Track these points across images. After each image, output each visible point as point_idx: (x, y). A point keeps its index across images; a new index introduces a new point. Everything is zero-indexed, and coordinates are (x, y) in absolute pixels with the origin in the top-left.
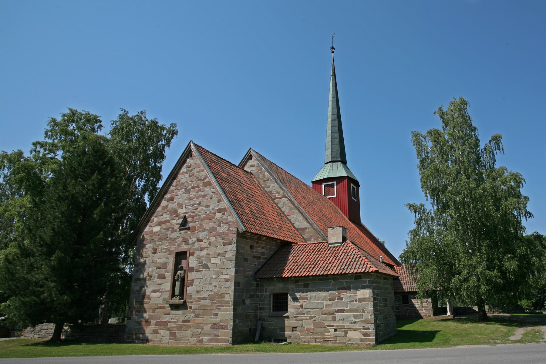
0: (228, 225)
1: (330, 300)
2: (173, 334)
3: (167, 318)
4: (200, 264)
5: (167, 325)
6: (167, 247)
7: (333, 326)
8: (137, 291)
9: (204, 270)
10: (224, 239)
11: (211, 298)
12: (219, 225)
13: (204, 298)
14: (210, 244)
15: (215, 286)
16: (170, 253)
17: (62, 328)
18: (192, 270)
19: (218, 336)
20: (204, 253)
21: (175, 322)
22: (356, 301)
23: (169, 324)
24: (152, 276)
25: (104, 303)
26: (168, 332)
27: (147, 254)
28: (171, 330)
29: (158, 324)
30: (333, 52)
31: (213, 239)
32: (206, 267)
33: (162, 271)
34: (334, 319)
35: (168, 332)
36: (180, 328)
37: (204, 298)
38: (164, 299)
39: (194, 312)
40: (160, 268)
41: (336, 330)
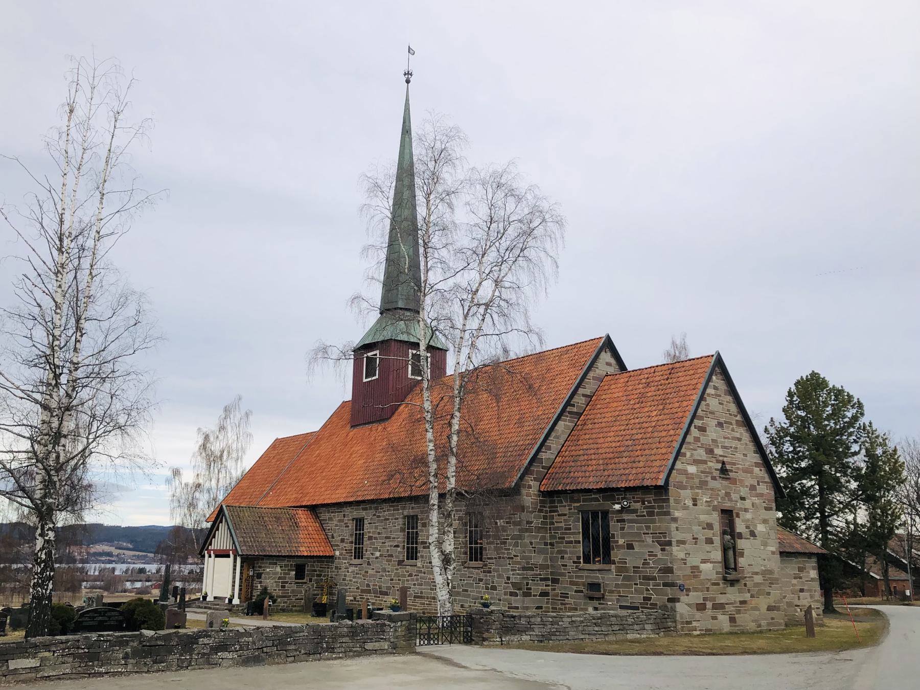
1: (795, 578)
2: (732, 620)
3: (722, 599)
5: (724, 608)
7: (799, 606)
13: (757, 573)
14: (753, 505)
15: (765, 560)
16: (715, 509)
18: (740, 536)
20: (749, 516)
21: (732, 604)
23: (727, 606)
24: (697, 538)
26: (727, 617)
28: (730, 614)
32: (753, 534)
36: (739, 612)
37: (757, 573)
38: (717, 573)
39: (749, 591)
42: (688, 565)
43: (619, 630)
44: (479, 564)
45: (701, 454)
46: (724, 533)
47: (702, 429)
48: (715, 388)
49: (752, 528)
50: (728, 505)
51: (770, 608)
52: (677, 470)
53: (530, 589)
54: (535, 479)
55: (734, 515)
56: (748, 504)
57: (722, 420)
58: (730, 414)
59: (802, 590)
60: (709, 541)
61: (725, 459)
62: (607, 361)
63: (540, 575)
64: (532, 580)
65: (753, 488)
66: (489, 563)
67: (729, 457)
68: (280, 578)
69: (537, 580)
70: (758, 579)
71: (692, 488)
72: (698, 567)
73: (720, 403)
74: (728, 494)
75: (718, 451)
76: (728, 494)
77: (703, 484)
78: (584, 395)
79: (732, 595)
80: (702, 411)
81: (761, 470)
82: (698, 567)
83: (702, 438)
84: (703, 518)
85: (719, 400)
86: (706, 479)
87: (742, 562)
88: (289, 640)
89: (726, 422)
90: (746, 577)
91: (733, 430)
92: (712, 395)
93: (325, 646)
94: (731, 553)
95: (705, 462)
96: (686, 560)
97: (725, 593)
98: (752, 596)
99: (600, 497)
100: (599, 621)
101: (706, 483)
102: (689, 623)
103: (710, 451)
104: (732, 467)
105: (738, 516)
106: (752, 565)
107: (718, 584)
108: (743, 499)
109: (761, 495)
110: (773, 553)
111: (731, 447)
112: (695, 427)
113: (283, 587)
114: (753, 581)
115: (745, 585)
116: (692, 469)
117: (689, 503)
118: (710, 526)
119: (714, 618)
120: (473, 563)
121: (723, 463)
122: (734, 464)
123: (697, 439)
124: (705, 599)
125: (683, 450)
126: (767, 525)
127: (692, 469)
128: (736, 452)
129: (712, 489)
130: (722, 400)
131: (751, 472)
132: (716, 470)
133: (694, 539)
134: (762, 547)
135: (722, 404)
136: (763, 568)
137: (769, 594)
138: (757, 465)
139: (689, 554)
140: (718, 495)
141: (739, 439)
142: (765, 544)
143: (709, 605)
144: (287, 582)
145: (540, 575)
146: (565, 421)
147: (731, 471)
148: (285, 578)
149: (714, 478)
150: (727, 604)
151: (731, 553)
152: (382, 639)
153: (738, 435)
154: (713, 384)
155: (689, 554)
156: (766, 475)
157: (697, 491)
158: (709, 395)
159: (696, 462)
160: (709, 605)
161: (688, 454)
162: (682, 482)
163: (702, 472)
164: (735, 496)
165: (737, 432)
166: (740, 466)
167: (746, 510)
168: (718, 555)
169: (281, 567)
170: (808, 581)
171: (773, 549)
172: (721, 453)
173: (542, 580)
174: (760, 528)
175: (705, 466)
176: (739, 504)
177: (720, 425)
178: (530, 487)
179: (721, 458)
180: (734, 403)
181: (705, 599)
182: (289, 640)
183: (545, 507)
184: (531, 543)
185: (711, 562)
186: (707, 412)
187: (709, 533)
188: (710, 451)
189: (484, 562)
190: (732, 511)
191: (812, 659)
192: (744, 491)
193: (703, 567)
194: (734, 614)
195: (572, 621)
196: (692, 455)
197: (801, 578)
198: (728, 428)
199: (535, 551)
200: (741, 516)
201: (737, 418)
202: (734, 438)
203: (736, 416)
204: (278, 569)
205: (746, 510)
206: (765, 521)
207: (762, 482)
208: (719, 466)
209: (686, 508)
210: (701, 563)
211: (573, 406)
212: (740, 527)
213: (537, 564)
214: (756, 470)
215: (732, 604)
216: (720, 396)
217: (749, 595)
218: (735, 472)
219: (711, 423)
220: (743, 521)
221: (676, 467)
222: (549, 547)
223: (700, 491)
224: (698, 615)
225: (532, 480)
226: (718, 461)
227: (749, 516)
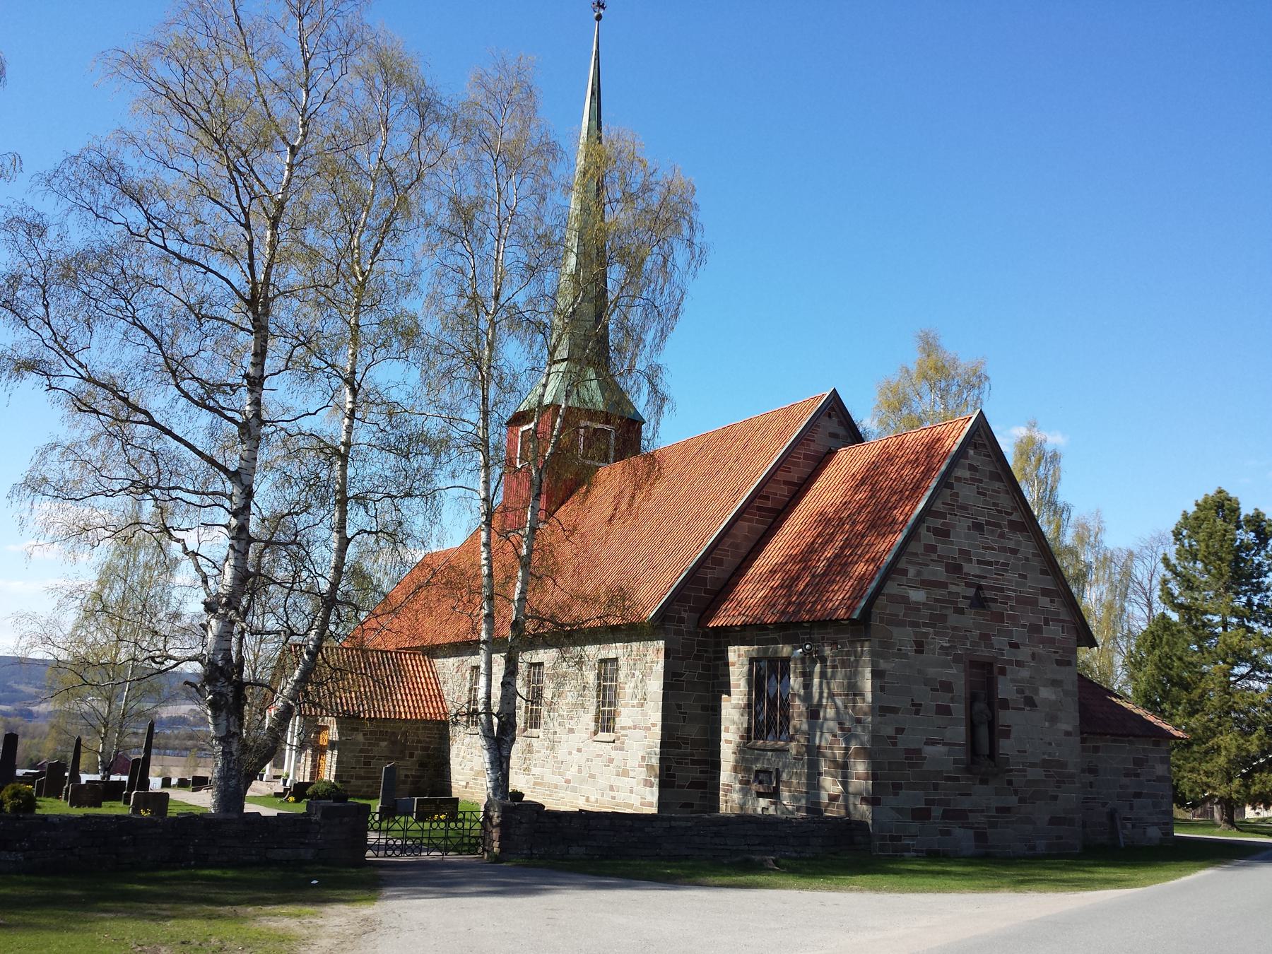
0: (1063, 626)
1: (1127, 775)
3: (965, 804)
4: (1019, 696)
6: (948, 645)
7: (1130, 819)
8: (889, 737)
9: (1028, 709)
10: (1057, 652)
11: (1046, 764)
12: (1047, 623)
13: (1033, 765)
14: (1033, 656)
15: (1050, 744)
16: (957, 659)
17: (744, 821)
18: (1005, 704)
19: (1061, 838)
20: (1024, 673)
22: (1154, 781)
25: (1242, 773)
26: (971, 832)
27: (900, 650)
28: (978, 828)
29: (949, 815)
30: (599, 18)
31: (1040, 650)
32: (1030, 702)
33: (944, 699)
34: (1131, 807)
35: (971, 832)
37: (1033, 765)
39: (1016, 792)
40: (938, 690)
41: (1133, 826)
42: (900, 746)
43: (759, 844)
44: (611, 736)
45: (938, 572)
46: (972, 699)
47: (944, 533)
48: (972, 468)
49: (1027, 693)
50: (983, 653)
51: (1054, 821)
52: (889, 595)
53: (674, 776)
54: (692, 610)
55: (996, 670)
56: (1024, 653)
57: (982, 519)
58: (1000, 512)
59: (1138, 795)
60: (944, 710)
61: (983, 582)
62: (831, 430)
63: (692, 755)
64: (677, 763)
65: (1035, 629)
66: (623, 736)
67: (993, 579)
68: (361, 751)
69: (687, 764)
70: (1035, 774)
71: (915, 625)
72: (918, 751)
73: (979, 493)
74: (985, 637)
75: (971, 569)
76: (985, 637)
77: (937, 621)
78: (786, 483)
79: (983, 798)
80: (943, 503)
81: (1052, 601)
82: (918, 751)
83: (940, 546)
84: (932, 672)
85: (978, 488)
86: (944, 612)
87: (1006, 747)
88: (124, 838)
89: (988, 523)
90: (1011, 771)
91: (1002, 536)
92: (965, 479)
93: (192, 851)
94: (983, 732)
95: (944, 585)
96: (896, 738)
97: (970, 795)
98: (1022, 800)
99: (779, 636)
100: (724, 828)
101: (943, 618)
102: (899, 838)
103: (955, 569)
104: (996, 595)
105: (1003, 671)
106: (1025, 752)
107: (957, 779)
108: (1014, 646)
109: (1051, 641)
110: (1068, 734)
111: (997, 563)
112: (929, 529)
113: (369, 763)
114: (1025, 776)
115: (1010, 782)
116: (917, 596)
117: (909, 649)
118: (947, 687)
119: (947, 833)
120: (603, 736)
121: (979, 587)
122: (1002, 590)
123: (931, 549)
124: (928, 802)
125: (902, 565)
126: (1060, 689)
127: (917, 596)
128: (1007, 571)
129: (955, 628)
130: (985, 489)
131: (1034, 603)
132: (964, 597)
133: (913, 705)
134: (1047, 724)
135: (985, 495)
136: (1046, 757)
137: (1055, 798)
138: (1045, 592)
139: (903, 730)
140: (966, 637)
141: (1014, 551)
142: (1053, 719)
143: (937, 811)
144: (373, 758)
145: (692, 755)
146: (751, 521)
147: (995, 601)
148: (368, 751)
149: (960, 611)
150: (971, 811)
151: (983, 732)
152: (302, 844)
153: (1012, 545)
154: (968, 462)
155: (903, 730)
156: (1062, 610)
157: (924, 630)
158: (958, 479)
159: (926, 584)
160: (937, 811)
161: (912, 571)
162: (898, 616)
163: (937, 600)
164: (999, 641)
165: (1009, 539)
166: (1014, 594)
167: (1019, 664)
168: (959, 733)
169: (364, 735)
170: (1149, 781)
171: (1069, 728)
172: (978, 573)
173: (694, 762)
174: (1045, 693)
175: (943, 592)
176: (1008, 654)
177: (978, 527)
178: (681, 620)
179: (976, 581)
180: (1007, 492)
181: (928, 802)
182: (124, 838)
183: (706, 651)
184: (679, 707)
185: (945, 744)
186: (954, 505)
187: (944, 699)
188: (955, 569)
189: (616, 733)
190: (991, 665)
191: (347, 907)
192: (1018, 634)
193: (929, 750)
194: (986, 829)
195: (671, 827)
196: (919, 573)
197: (1137, 775)
198: (992, 531)
199: (684, 719)
200: (1008, 672)
201: (1010, 518)
202: (1002, 549)
203: (1011, 514)
204: (360, 737)
205: (1019, 664)
206: (1055, 683)
207: (1052, 620)
208: (971, 592)
209: (901, 655)
210: (926, 744)
211: (767, 498)
212: (1005, 689)
213: (688, 739)
214: (1044, 602)
215: (983, 811)
216: (981, 481)
217: (1015, 799)
218: (1001, 603)
219: (961, 526)
220: (1013, 681)
221: (885, 591)
222: (710, 712)
223: (931, 630)
224: (914, 827)
225: (685, 611)
226: (968, 585)
227: (1024, 673)
